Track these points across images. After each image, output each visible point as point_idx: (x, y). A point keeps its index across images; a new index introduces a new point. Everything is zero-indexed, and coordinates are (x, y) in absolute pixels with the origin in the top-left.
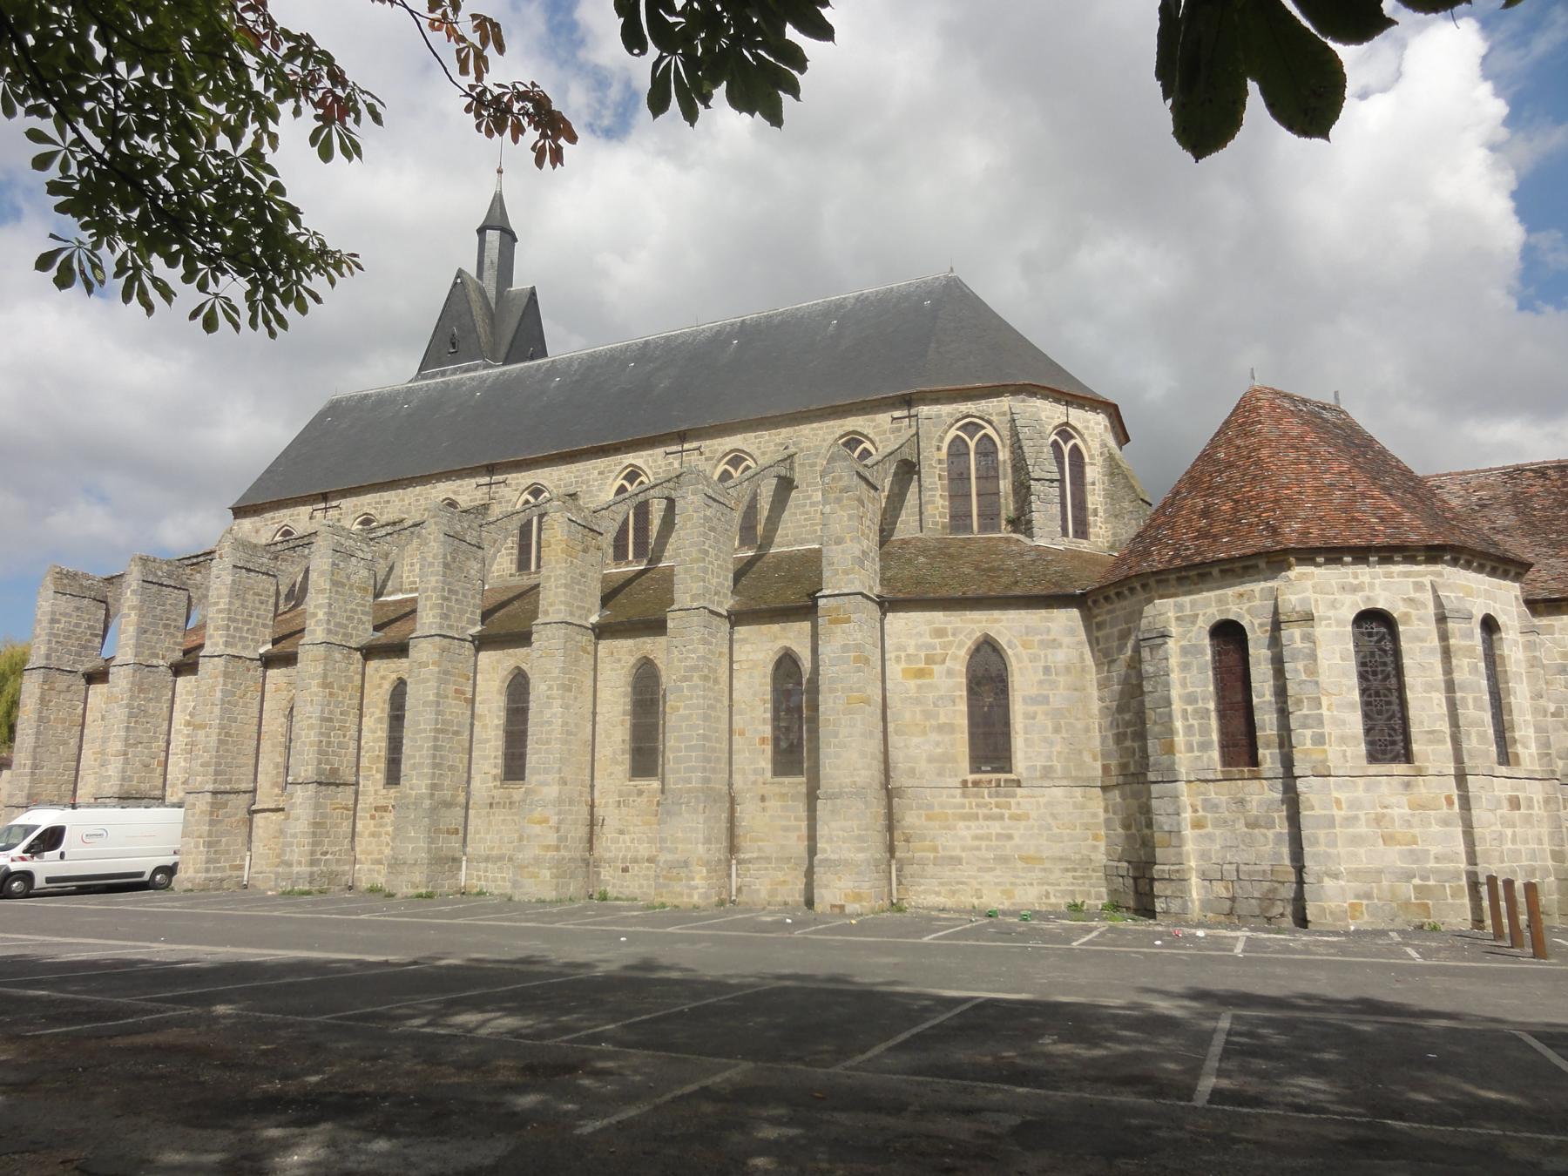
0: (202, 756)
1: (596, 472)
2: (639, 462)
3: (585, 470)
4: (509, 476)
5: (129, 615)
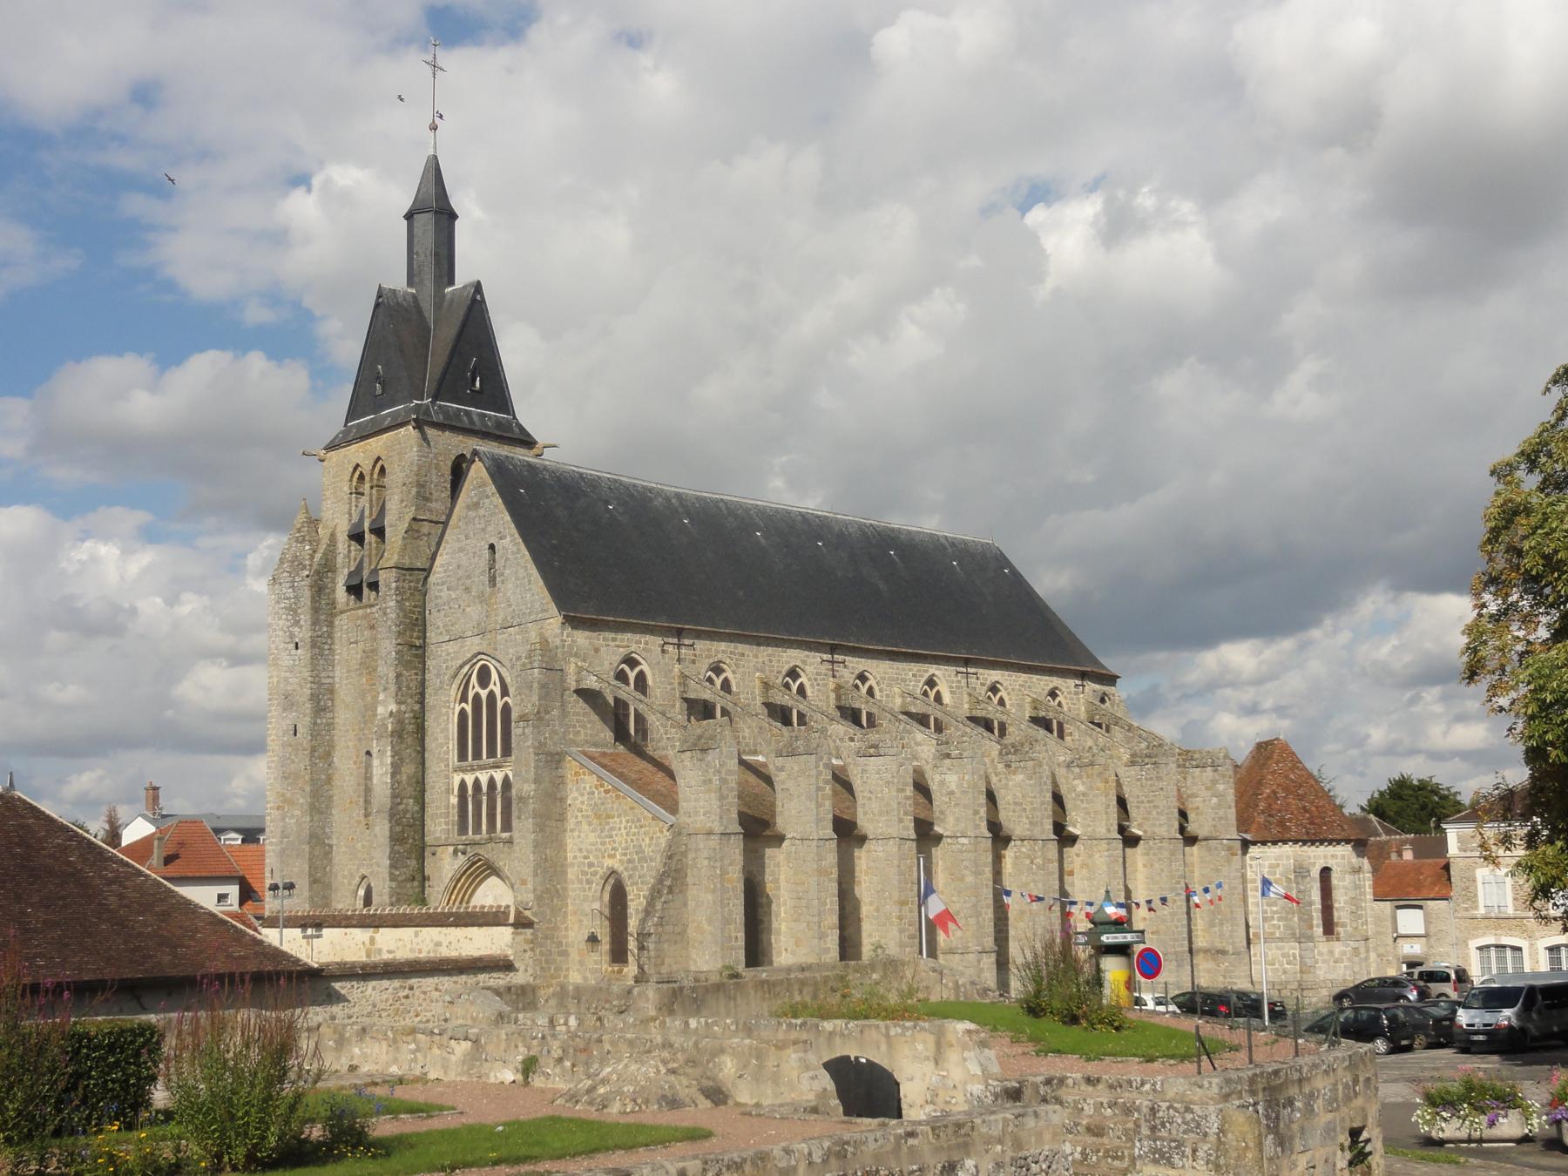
0: (908, 930)
1: (910, 674)
2: (937, 673)
3: (904, 670)
4: (847, 658)
5: (824, 789)
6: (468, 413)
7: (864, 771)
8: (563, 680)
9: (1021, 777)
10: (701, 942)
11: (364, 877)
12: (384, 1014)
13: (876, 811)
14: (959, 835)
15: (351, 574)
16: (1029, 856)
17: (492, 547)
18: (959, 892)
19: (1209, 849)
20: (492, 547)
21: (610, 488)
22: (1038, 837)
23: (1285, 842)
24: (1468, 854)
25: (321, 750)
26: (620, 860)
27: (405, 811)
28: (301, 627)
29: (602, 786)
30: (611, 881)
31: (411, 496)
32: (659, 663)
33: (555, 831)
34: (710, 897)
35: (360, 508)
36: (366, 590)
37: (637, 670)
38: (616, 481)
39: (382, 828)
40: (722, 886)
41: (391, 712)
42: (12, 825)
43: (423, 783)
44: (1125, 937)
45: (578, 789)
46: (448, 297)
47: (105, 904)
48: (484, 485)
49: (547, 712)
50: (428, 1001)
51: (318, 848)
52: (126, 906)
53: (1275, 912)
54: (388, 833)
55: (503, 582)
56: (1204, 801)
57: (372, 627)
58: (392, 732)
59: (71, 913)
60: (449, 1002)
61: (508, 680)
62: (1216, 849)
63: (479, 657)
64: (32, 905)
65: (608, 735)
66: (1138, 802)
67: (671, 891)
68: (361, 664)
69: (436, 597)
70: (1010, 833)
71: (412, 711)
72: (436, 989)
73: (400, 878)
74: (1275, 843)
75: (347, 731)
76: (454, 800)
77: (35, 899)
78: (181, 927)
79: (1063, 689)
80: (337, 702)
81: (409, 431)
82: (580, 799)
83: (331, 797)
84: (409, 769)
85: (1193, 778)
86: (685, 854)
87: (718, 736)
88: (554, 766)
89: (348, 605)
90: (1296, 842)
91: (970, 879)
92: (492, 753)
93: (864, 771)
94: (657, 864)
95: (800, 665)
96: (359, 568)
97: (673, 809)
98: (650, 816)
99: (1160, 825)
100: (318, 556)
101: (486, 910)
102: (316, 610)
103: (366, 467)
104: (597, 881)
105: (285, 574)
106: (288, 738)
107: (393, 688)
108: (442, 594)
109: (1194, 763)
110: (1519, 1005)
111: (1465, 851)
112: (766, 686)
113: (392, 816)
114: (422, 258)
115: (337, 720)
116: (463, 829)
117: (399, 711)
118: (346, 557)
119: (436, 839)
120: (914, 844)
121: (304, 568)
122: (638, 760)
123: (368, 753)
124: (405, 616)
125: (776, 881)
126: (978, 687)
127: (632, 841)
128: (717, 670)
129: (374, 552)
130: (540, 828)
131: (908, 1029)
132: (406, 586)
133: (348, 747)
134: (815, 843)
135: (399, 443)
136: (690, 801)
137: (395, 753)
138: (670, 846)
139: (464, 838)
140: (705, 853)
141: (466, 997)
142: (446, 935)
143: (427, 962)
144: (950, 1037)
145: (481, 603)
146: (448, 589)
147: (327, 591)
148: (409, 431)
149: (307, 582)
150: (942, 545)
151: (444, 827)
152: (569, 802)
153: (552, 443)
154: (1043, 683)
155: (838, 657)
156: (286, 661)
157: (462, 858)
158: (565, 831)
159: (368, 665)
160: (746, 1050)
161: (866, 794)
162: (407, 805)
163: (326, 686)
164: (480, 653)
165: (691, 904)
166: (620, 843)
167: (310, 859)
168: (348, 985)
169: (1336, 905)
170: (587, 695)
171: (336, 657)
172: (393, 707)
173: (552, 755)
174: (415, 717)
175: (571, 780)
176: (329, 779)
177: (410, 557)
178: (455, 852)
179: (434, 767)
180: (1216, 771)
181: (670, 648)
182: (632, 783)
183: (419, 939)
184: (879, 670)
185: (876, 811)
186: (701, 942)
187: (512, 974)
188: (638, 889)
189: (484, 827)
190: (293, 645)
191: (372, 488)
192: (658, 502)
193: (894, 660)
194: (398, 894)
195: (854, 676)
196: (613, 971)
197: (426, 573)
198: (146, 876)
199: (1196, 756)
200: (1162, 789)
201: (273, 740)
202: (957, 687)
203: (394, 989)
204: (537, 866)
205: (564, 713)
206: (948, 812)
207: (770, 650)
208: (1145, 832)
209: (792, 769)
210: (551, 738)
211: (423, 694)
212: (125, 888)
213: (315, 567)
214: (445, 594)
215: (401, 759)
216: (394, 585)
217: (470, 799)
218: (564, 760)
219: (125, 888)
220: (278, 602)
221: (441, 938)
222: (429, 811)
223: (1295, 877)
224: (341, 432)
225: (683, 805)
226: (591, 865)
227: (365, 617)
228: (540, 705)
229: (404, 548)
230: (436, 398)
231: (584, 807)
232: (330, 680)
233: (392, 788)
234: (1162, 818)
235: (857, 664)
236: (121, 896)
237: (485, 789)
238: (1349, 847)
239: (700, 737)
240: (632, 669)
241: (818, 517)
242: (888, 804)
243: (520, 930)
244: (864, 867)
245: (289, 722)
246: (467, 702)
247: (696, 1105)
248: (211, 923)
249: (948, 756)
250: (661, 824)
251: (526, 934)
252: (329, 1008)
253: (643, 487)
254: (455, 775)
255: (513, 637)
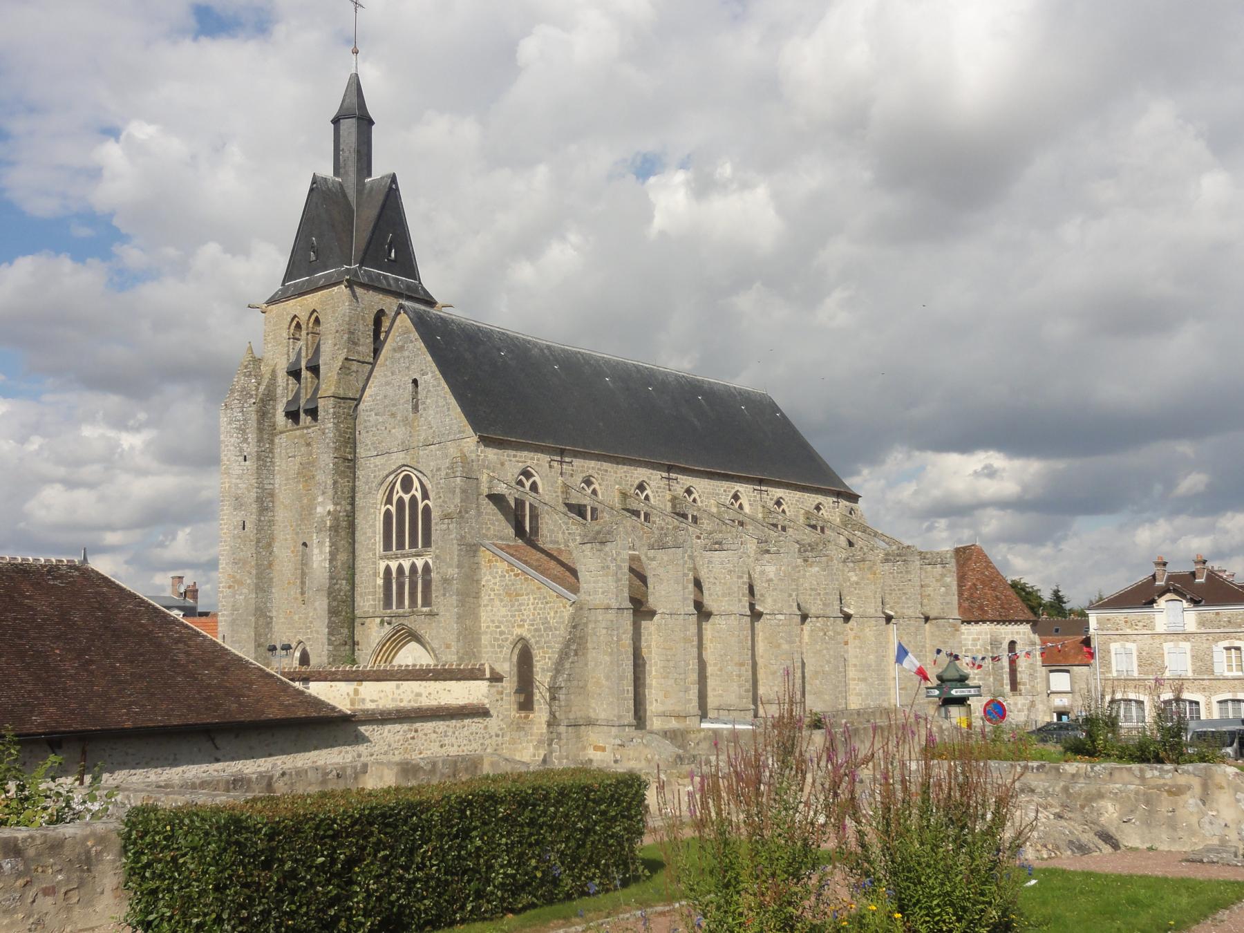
1: (722, 489)
2: (740, 489)
4: (679, 476)
6: (385, 277)
7: (710, 562)
8: (478, 487)
9: (817, 569)
10: (600, 694)
11: (300, 642)
12: (396, 752)
13: (720, 593)
14: (776, 612)
15: (289, 403)
16: (823, 630)
17: (415, 382)
18: (777, 656)
19: (938, 626)
20: (415, 382)
21: (500, 339)
22: (830, 615)
23: (984, 622)
24: (1105, 632)
25: (264, 542)
26: (528, 630)
27: (340, 590)
28: (249, 444)
29: (512, 570)
30: (519, 646)
31: (343, 341)
32: (547, 476)
33: (472, 606)
34: (607, 658)
35: (297, 349)
36: (302, 415)
37: (531, 481)
38: (503, 334)
39: (321, 604)
40: (618, 650)
41: (329, 512)
42: (91, 593)
43: (354, 568)
44: (970, 691)
45: (490, 574)
46: (368, 186)
47: (176, 660)
48: (407, 332)
49: (467, 512)
50: (428, 741)
51: (261, 619)
52: (193, 662)
53: (977, 674)
54: (326, 607)
55: (425, 409)
56: (935, 590)
57: (308, 445)
58: (330, 527)
59: (151, 668)
60: (620, 745)
61: (429, 486)
62: (944, 626)
63: (403, 469)
64: (119, 661)
65: (511, 531)
66: (891, 590)
67: (576, 654)
68: (298, 473)
69: (365, 421)
70: (807, 612)
71: (345, 511)
72: (434, 732)
73: (335, 643)
74: (977, 622)
75: (286, 527)
76: (380, 582)
77: (121, 655)
78: (239, 680)
79: (825, 505)
80: (277, 504)
81: (342, 289)
82: (493, 581)
83: (272, 578)
84: (342, 557)
85: (926, 572)
86: (586, 624)
87: (615, 532)
88: (472, 555)
89: (286, 426)
90: (992, 621)
91: (785, 647)
92: (413, 544)
93: (710, 562)
94: (563, 632)
95: (646, 479)
96: (297, 397)
97: (575, 590)
98: (556, 594)
99: (908, 608)
100: (262, 388)
101: (410, 668)
102: (260, 430)
103: (303, 317)
104: (508, 645)
105: (236, 401)
106: (238, 531)
107: (330, 492)
108: (371, 418)
109: (927, 561)
110: (1235, 744)
111: (1102, 630)
112: (624, 495)
113: (329, 594)
114: (347, 154)
115: (276, 518)
116: (387, 603)
117: (335, 510)
118: (285, 388)
119: (364, 612)
120: (749, 618)
121: (251, 396)
122: (534, 551)
123: (305, 544)
124: (340, 436)
125: (649, 647)
126: (768, 500)
127: (539, 614)
128: (588, 482)
129: (309, 385)
130: (462, 603)
131: (1168, 771)
132: (341, 411)
133: (286, 540)
134: (682, 617)
135: (333, 299)
136: (590, 583)
137: (332, 544)
138: (574, 619)
139: (389, 611)
140: (604, 625)
141: (640, 740)
142: (425, 687)
143: (427, 710)
144: (1219, 779)
145: (405, 425)
146: (376, 415)
147: (270, 415)
148: (342, 289)
149: (254, 408)
150: (732, 393)
151: (372, 603)
152: (483, 583)
153: (449, 304)
154: (811, 499)
155: (673, 475)
156: (236, 470)
157: (387, 628)
158: (480, 606)
159: (306, 473)
160: (1132, 796)
161: (712, 580)
162: (341, 585)
163: (268, 491)
164: (404, 465)
165: (591, 664)
166: (529, 615)
167: (256, 628)
168: (370, 728)
169: (1019, 669)
170: (497, 499)
171: (276, 468)
172: (331, 507)
173: (470, 546)
174: (347, 516)
175: (485, 566)
176: (270, 565)
177: (343, 389)
178: (382, 622)
179: (362, 555)
180: (944, 567)
181: (555, 464)
182: (536, 569)
183: (400, 691)
184: (701, 486)
185: (720, 593)
186: (600, 694)
187: (488, 719)
188: (544, 652)
189: (407, 602)
190: (242, 458)
191: (308, 334)
192: (535, 351)
193: (711, 479)
194: (334, 655)
195: (683, 490)
196: (520, 717)
197: (356, 402)
198: (203, 636)
199: (928, 556)
200: (910, 580)
201: (225, 533)
202: (754, 501)
203: (405, 732)
204: (459, 634)
205: (479, 513)
206: (767, 595)
207: (626, 468)
208: (896, 612)
209: (662, 559)
210: (469, 533)
211: (353, 498)
212: (189, 647)
213: (260, 396)
214: (373, 418)
215: (337, 549)
216: (332, 410)
217: (394, 581)
218: (479, 551)
219: (189, 647)
220: (230, 424)
221: (422, 690)
222: (358, 590)
223: (992, 648)
224: (279, 290)
225: (584, 586)
226: (502, 633)
227: (302, 436)
228: (462, 506)
229: (339, 381)
230: (362, 264)
231: (496, 587)
232: (271, 486)
233: (330, 571)
234: (909, 602)
235: (686, 481)
236: (187, 654)
237: (407, 572)
238: (1028, 626)
239: (598, 533)
240: (528, 479)
241: (647, 368)
242: (730, 588)
243: (494, 684)
244: (710, 637)
245: (238, 518)
246: (392, 505)
247: (1101, 850)
248: (261, 676)
249: (768, 552)
250: (565, 600)
251: (498, 686)
252: (356, 748)
253: (523, 339)
254: (381, 562)
255: (433, 453)
